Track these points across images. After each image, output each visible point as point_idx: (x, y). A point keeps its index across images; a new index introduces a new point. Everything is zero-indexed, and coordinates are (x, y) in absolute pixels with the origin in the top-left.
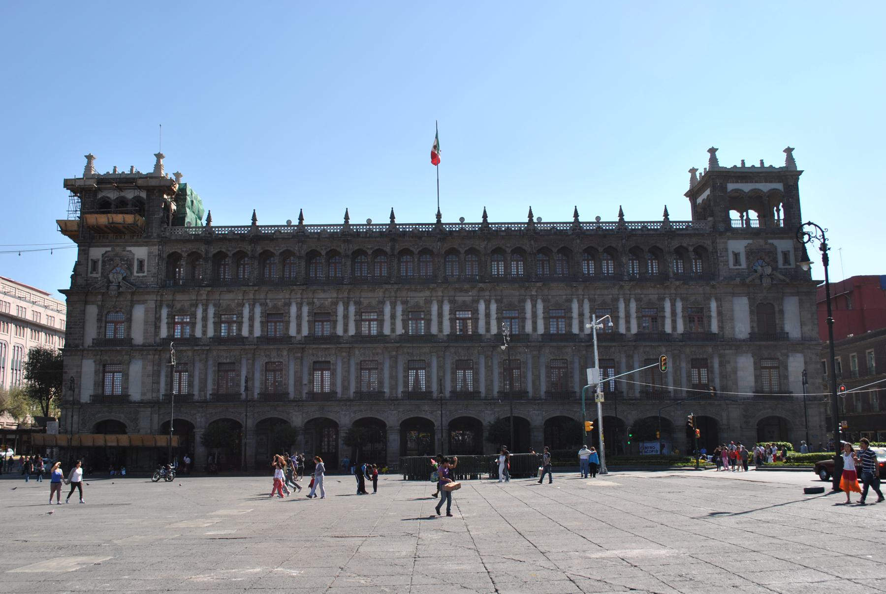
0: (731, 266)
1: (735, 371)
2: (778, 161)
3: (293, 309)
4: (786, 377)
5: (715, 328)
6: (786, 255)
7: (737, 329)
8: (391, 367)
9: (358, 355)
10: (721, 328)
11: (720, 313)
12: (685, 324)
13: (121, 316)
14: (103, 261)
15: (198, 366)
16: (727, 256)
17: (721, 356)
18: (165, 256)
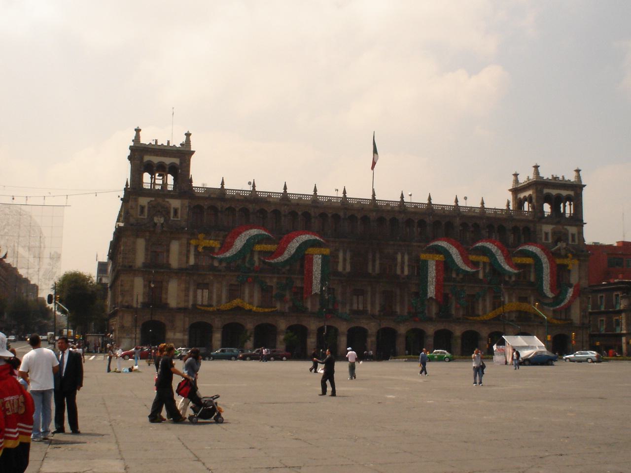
2: (571, 177)
14: (149, 208)
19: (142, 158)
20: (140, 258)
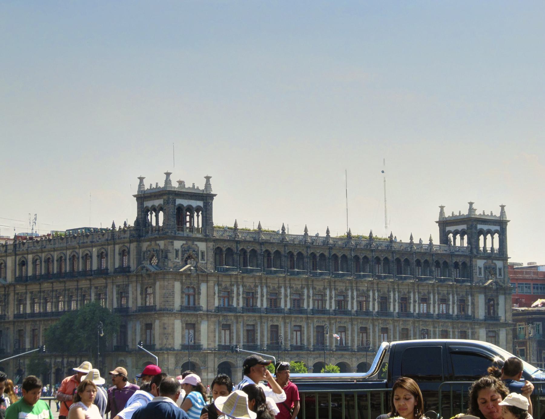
5: (470, 313)
14: (182, 251)
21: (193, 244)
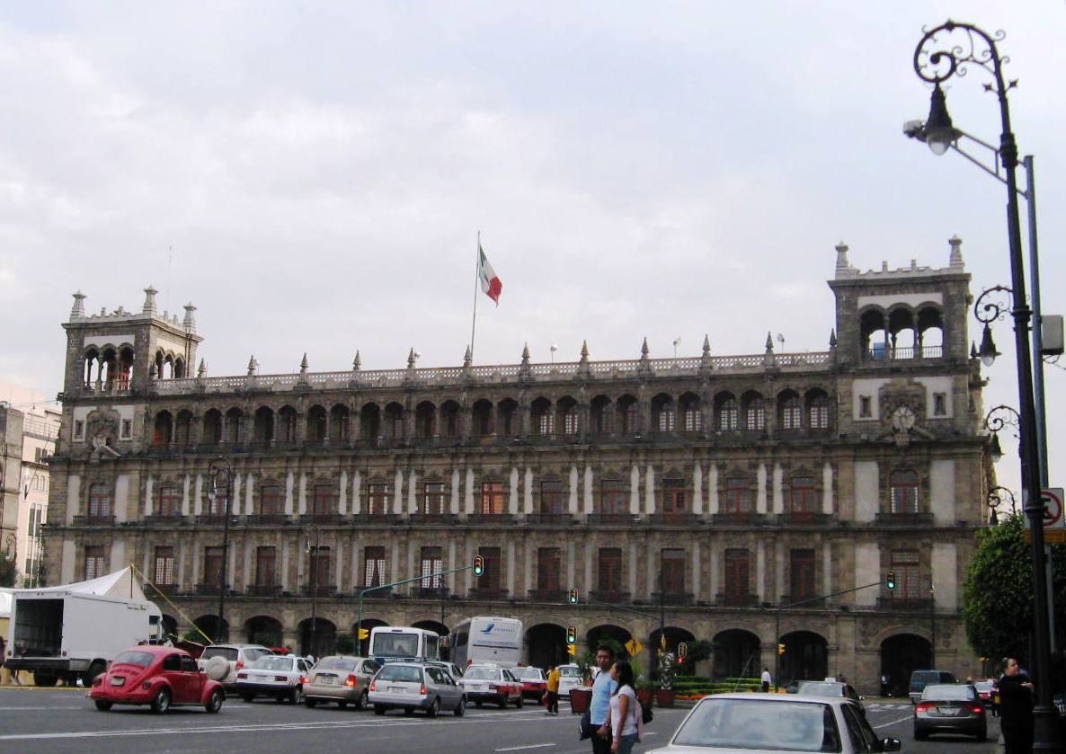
0: (857, 417)
1: (852, 568)
2: (938, 261)
3: (290, 482)
4: (929, 578)
5: (828, 508)
6: (939, 398)
7: (859, 508)
8: (400, 556)
9: (362, 541)
10: (836, 508)
11: (835, 486)
12: (785, 502)
13: (105, 490)
14: (89, 424)
15: (184, 551)
16: (851, 403)
17: (834, 547)
18: (153, 416)
19: (82, 343)
20: (74, 509)
21: (110, 410)
